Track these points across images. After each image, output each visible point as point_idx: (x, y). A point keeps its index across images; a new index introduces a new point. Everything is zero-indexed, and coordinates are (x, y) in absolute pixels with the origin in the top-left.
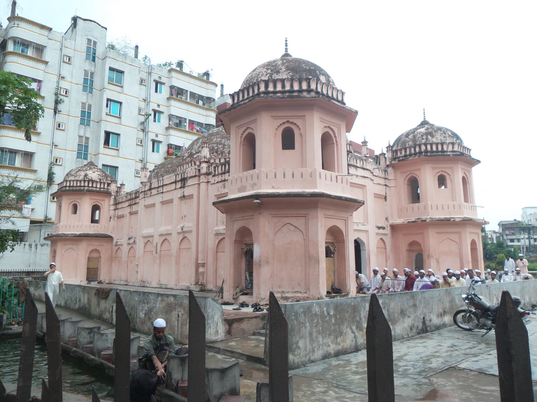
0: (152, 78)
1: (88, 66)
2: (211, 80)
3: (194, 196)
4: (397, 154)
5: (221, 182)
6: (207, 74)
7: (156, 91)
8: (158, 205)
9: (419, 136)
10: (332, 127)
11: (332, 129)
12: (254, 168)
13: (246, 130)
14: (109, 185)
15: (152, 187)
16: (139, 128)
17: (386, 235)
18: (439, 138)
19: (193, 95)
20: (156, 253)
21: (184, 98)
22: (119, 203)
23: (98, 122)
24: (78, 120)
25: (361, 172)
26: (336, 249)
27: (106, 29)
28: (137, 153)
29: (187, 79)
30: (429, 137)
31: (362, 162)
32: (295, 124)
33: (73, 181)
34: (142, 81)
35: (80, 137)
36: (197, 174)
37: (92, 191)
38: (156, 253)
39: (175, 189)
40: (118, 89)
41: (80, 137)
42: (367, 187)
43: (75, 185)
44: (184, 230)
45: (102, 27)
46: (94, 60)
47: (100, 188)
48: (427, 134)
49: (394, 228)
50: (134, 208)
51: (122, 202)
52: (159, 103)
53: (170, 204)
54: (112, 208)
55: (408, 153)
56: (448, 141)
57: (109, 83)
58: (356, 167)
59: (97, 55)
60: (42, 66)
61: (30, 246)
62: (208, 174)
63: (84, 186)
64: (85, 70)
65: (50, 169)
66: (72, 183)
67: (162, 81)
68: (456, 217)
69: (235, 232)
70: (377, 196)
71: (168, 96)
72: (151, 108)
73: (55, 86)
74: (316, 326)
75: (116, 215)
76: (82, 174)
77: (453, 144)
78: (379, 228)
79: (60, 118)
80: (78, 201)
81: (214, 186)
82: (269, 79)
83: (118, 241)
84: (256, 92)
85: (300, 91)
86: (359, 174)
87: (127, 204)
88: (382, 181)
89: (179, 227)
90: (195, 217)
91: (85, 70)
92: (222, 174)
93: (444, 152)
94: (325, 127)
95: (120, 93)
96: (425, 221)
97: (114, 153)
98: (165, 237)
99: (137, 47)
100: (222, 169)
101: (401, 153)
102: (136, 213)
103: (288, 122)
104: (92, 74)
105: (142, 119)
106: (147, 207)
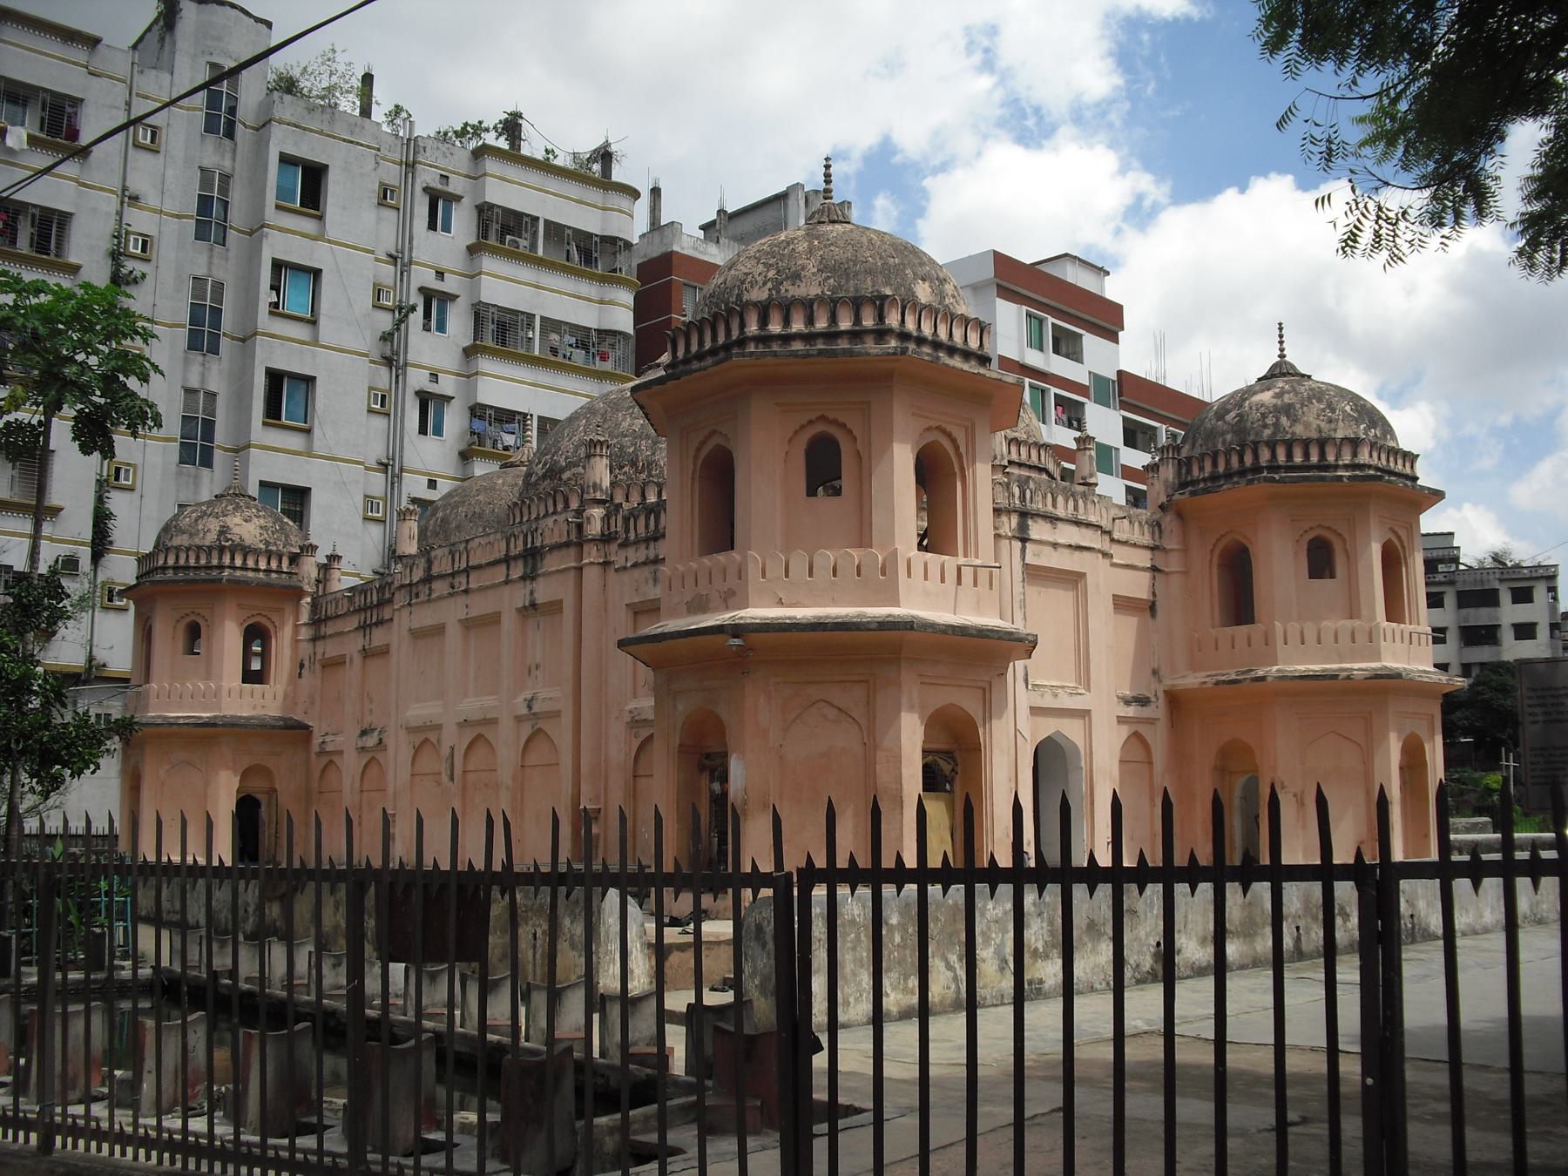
0: (418, 181)
1: (213, 155)
2: (617, 175)
3: (565, 605)
4: (1189, 471)
5: (644, 563)
6: (605, 156)
7: (432, 226)
8: (453, 633)
9: (1256, 415)
10: (949, 428)
11: (949, 435)
12: (731, 545)
13: (708, 438)
14: (294, 559)
15: (435, 570)
17: (1150, 721)
18: (1315, 423)
19: (555, 231)
20: (452, 779)
21: (523, 243)
22: (328, 618)
23: (243, 340)
24: (183, 334)
26: (959, 769)
27: (269, 25)
28: (370, 437)
29: (534, 177)
30: (1284, 420)
31: (1071, 503)
32: (843, 426)
33: (188, 549)
34: (385, 195)
35: (189, 391)
36: (573, 537)
38: (452, 779)
39: (507, 582)
40: (308, 225)
41: (189, 391)
42: (1089, 578)
43: (192, 562)
44: (536, 708)
46: (230, 134)
47: (268, 571)
48: (1278, 410)
49: (1175, 700)
50: (378, 637)
51: (338, 616)
54: (305, 634)
55: (1221, 469)
56: (1340, 435)
57: (278, 207)
58: (1053, 519)
59: (240, 114)
64: (202, 169)
65: (100, 499)
66: (183, 556)
67: (450, 189)
68: (1356, 666)
70: (1123, 604)
71: (472, 240)
72: (415, 284)
73: (111, 225)
74: (854, 949)
75: (319, 656)
76: (214, 525)
77: (1355, 443)
80: (203, 612)
81: (625, 577)
82: (770, 295)
83: (328, 739)
84: (735, 334)
85: (856, 335)
86: (1061, 541)
87: (354, 622)
88: (1143, 558)
89: (520, 699)
90: (568, 669)
91: (202, 169)
93: (1327, 468)
94: (929, 429)
95: (315, 239)
96: (1263, 679)
97: (295, 441)
98: (479, 733)
99: (368, 79)
100: (647, 526)
101: (1201, 469)
102: (384, 652)
103: (823, 418)
104: (226, 178)
105: (385, 321)
106: (417, 634)
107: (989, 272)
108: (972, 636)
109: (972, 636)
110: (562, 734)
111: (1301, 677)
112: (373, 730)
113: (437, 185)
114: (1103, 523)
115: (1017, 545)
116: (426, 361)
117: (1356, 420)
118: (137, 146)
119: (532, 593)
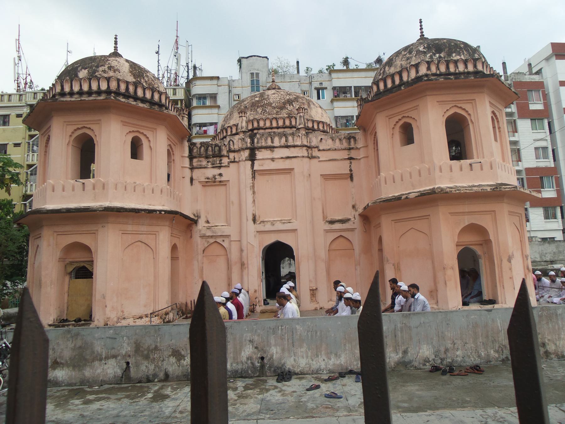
10: (88, 126)
11: (90, 128)
17: (352, 230)
21: (348, 95)
25: (280, 153)
27: (266, 57)
29: (356, 74)
31: (283, 139)
45: (263, 57)
58: (271, 148)
67: (323, 86)
70: (326, 177)
78: (332, 222)
86: (276, 157)
88: (345, 154)
94: (78, 129)
99: (298, 62)
107: (550, 51)
108: (64, 212)
109: (64, 212)
111: (384, 201)
113: (319, 86)
114: (313, 144)
115: (249, 163)
117: (424, 52)
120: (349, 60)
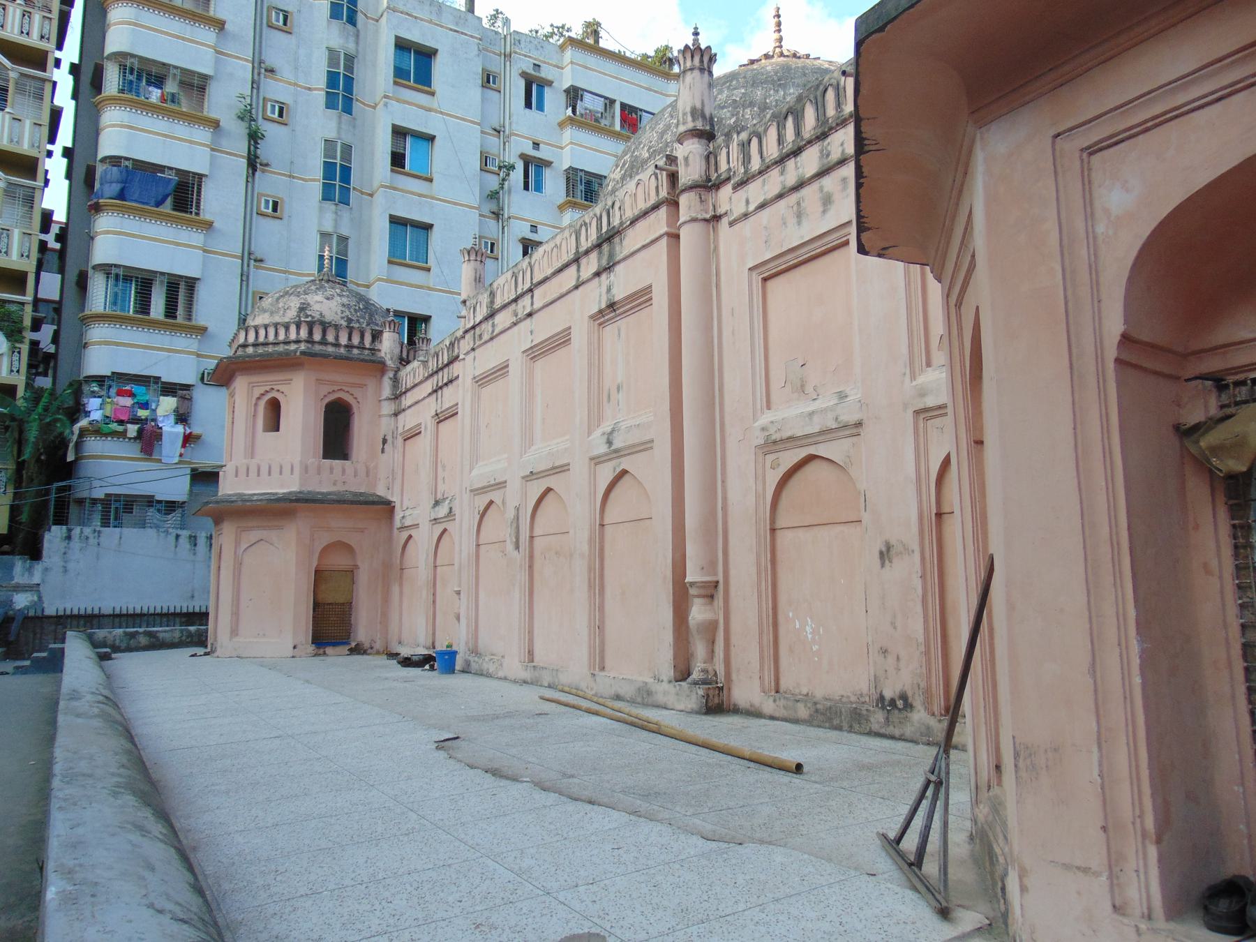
5: (780, 196)
14: (376, 336)
15: (498, 302)
16: (486, 212)
20: (517, 547)
22: (407, 391)
33: (266, 327)
34: (489, 80)
35: (325, 236)
36: (664, 193)
37: (325, 356)
38: (517, 547)
41: (325, 236)
43: (271, 338)
44: (618, 444)
47: (349, 347)
50: (449, 397)
52: (539, 138)
53: (562, 352)
54: (388, 408)
60: (207, 35)
61: (193, 540)
62: (709, 185)
63: (297, 342)
64: (330, 50)
66: (262, 332)
67: (543, 74)
69: (1121, 247)
75: (400, 430)
76: (295, 303)
79: (268, 184)
81: (746, 227)
87: (428, 386)
91: (330, 50)
92: (781, 161)
95: (429, 110)
100: (780, 140)
104: (350, 59)
105: (493, 182)
106: (482, 381)
110: (653, 472)
112: (444, 499)
116: (527, 215)
118: (270, 26)
119: (609, 290)
120: (602, 33)
